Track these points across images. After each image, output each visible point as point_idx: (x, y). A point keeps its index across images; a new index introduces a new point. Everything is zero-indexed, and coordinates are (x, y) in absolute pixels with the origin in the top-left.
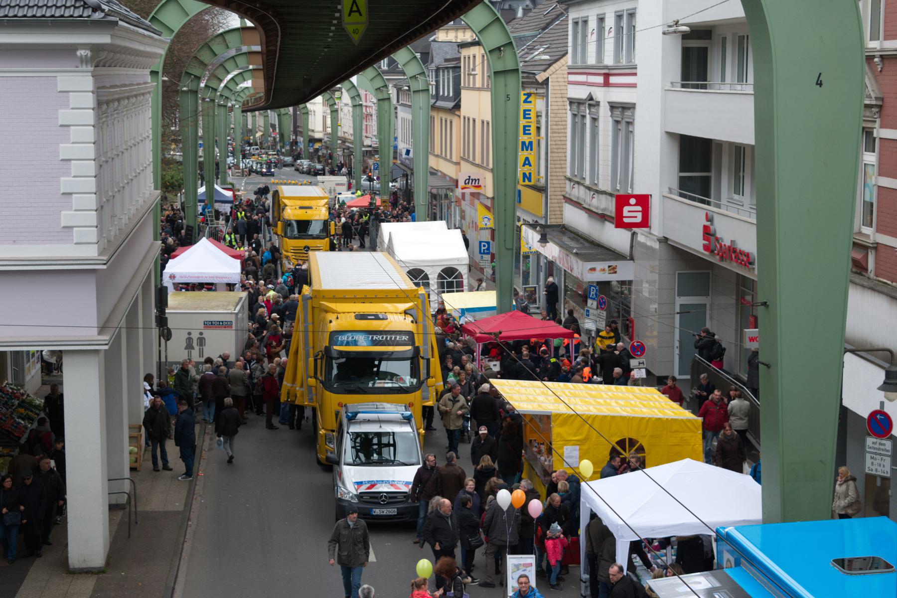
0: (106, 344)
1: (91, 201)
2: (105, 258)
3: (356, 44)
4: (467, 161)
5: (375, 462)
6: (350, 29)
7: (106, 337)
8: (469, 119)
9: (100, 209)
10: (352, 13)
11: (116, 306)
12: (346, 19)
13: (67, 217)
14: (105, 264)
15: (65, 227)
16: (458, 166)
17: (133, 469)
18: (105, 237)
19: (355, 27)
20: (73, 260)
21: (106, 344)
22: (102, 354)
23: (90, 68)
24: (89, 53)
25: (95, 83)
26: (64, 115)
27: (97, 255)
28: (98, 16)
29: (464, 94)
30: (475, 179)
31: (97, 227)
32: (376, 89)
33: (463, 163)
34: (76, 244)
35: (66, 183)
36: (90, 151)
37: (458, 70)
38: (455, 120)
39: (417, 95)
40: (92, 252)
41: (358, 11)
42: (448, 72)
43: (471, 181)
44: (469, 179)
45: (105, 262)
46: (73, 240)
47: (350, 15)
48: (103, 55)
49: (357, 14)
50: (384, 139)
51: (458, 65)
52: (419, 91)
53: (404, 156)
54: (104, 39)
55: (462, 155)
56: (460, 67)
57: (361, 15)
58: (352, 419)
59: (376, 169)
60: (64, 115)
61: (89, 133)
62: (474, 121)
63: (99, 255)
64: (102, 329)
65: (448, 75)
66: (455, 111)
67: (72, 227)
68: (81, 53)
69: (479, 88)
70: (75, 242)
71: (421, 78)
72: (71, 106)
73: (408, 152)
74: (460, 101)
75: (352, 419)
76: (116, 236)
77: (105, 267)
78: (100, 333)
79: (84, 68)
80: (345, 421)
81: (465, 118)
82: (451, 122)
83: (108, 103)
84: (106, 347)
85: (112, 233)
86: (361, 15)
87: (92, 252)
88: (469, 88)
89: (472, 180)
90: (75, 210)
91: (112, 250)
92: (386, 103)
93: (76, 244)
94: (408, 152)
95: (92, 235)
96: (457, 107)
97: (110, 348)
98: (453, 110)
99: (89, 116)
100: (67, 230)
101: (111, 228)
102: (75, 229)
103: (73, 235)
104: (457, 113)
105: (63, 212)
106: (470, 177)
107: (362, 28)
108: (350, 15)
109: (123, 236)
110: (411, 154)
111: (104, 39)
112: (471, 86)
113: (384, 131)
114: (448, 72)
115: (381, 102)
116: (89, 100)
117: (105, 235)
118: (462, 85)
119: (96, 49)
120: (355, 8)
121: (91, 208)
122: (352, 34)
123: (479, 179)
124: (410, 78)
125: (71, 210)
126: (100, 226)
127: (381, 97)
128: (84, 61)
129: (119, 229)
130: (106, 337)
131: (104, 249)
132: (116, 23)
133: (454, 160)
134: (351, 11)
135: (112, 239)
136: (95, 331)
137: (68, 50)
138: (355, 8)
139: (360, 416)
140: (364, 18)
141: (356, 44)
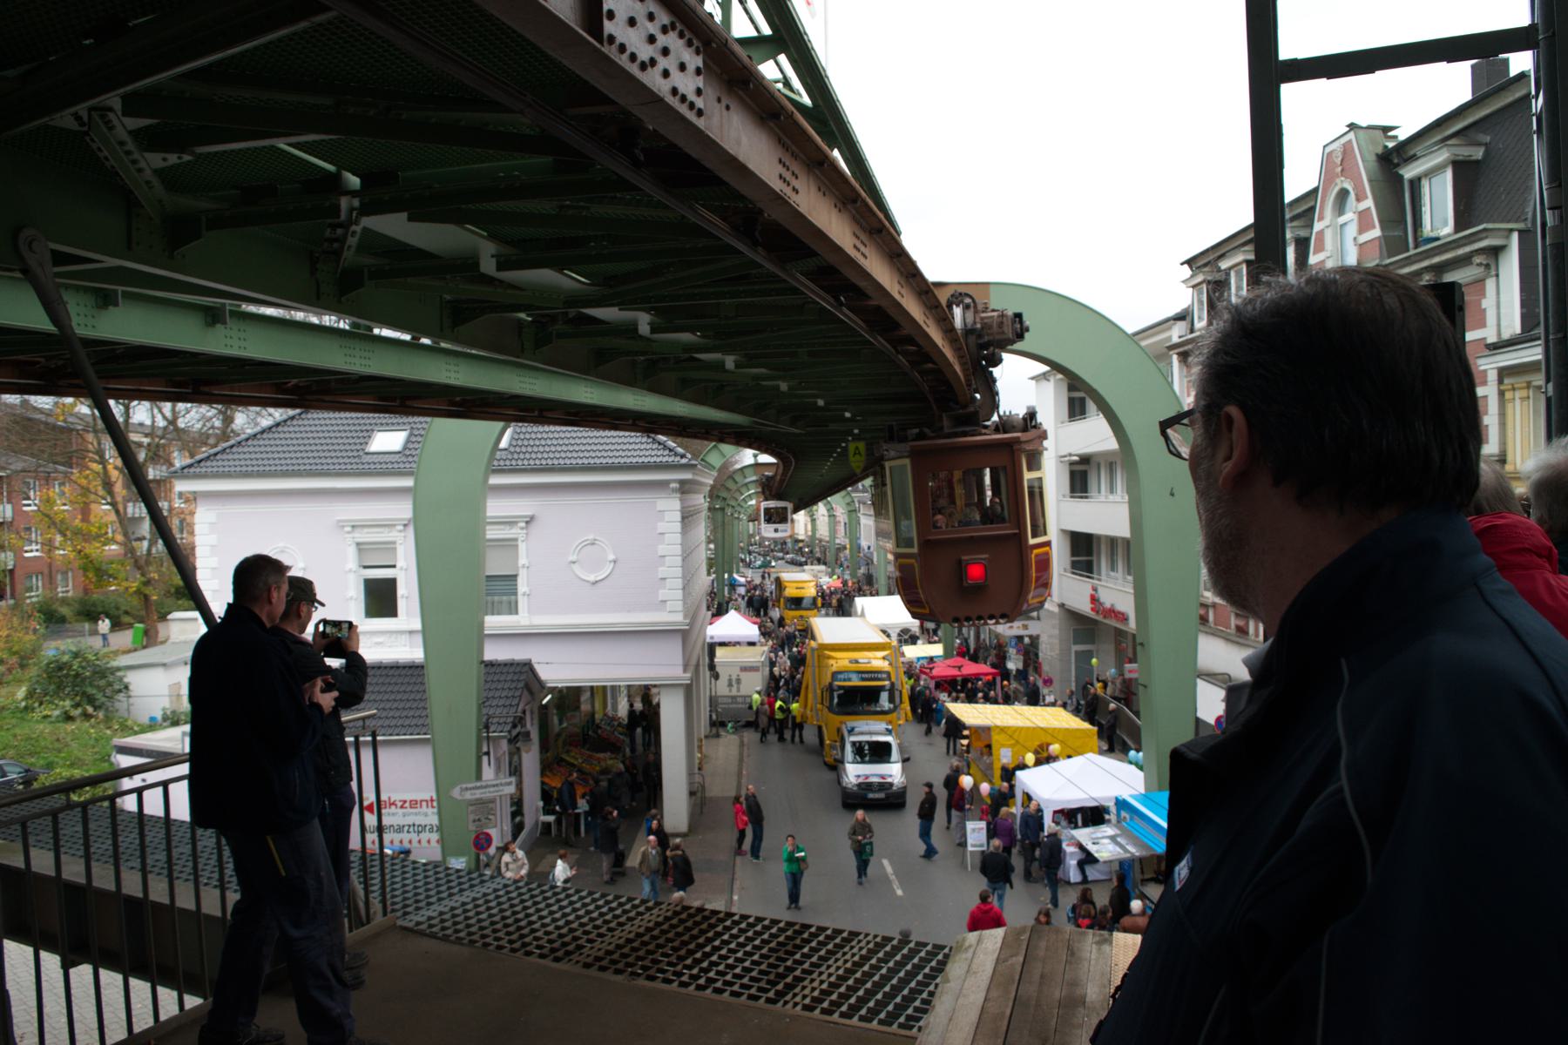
1: (679, 583)
9: (684, 589)
12: (852, 458)
13: (663, 594)
17: (700, 769)
23: (678, 495)
24: (678, 485)
25: (682, 504)
26: (662, 526)
28: (684, 461)
35: (662, 571)
36: (678, 550)
40: (679, 617)
41: (859, 453)
48: (687, 487)
54: (687, 476)
58: (851, 731)
60: (662, 526)
61: (678, 538)
68: (673, 485)
72: (666, 519)
73: (869, 548)
75: (851, 731)
79: (675, 495)
80: (846, 734)
83: (687, 517)
87: (679, 617)
94: (869, 548)
95: (679, 606)
99: (678, 527)
107: (862, 465)
110: (872, 549)
111: (687, 476)
116: (678, 516)
119: (682, 482)
126: (684, 600)
128: (674, 490)
130: (688, 675)
132: (696, 465)
134: (855, 454)
136: (681, 669)
137: (663, 485)
139: (856, 730)
140: (863, 458)
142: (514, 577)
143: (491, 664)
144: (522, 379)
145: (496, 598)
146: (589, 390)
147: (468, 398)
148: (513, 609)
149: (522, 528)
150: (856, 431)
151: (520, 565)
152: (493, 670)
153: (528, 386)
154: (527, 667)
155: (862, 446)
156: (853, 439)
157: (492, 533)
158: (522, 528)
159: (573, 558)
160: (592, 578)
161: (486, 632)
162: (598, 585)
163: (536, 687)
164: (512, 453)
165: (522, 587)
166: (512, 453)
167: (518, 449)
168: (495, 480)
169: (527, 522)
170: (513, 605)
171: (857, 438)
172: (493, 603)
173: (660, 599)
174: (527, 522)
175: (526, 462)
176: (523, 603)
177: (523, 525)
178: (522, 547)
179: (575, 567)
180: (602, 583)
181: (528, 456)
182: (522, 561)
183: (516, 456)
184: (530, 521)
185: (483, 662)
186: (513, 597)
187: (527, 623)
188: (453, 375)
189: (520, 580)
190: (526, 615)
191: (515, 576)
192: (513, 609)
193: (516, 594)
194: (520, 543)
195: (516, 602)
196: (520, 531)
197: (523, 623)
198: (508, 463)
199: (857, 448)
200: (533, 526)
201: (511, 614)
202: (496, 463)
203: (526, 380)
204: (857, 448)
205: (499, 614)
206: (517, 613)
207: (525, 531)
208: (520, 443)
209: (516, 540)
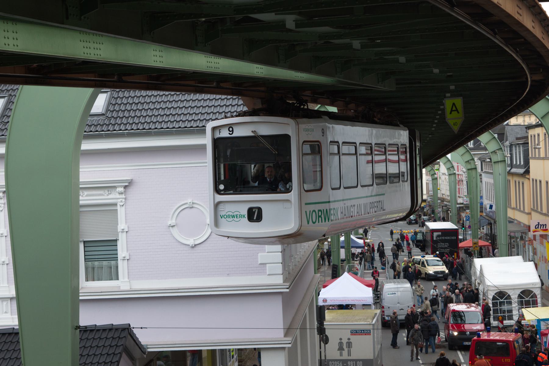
0: (289, 343)
2: (288, 284)
3: (456, 132)
4: (536, 211)
5: (525, 213)
6: (451, 122)
7: (289, 339)
8: (536, 181)
10: (453, 112)
11: (294, 318)
12: (448, 116)
14: (287, 288)
15: (261, 264)
16: (530, 216)
18: (286, 270)
19: (454, 121)
20: (267, 286)
21: (289, 343)
22: (287, 349)
27: (282, 282)
29: (532, 163)
30: (543, 225)
31: (282, 263)
32: (466, 162)
33: (533, 213)
34: (268, 275)
37: (526, 145)
38: (526, 182)
39: (497, 165)
40: (279, 280)
41: (457, 110)
42: (519, 147)
43: (540, 226)
44: (538, 225)
45: (288, 287)
46: (266, 272)
47: (451, 113)
49: (456, 112)
50: (473, 198)
51: (527, 142)
52: (498, 162)
53: (488, 210)
55: (532, 207)
56: (528, 143)
57: (458, 112)
59: (468, 220)
62: (540, 182)
63: (284, 283)
64: (288, 331)
65: (519, 149)
66: (525, 175)
67: (266, 264)
69: (543, 158)
70: (268, 273)
71: (499, 153)
73: (491, 207)
74: (529, 167)
76: (293, 269)
77: (288, 290)
78: (286, 335)
81: (533, 180)
82: (523, 184)
84: (290, 346)
85: (291, 268)
86: (458, 112)
88: (535, 158)
89: (541, 225)
90: (268, 252)
91: (292, 278)
92: (474, 171)
93: (268, 275)
94: (491, 207)
95: (279, 269)
96: (527, 172)
97: (292, 346)
98: (524, 174)
100: (262, 266)
101: (290, 264)
102: (267, 265)
103: (266, 269)
104: (527, 176)
105: (259, 254)
106: (539, 223)
107: (459, 122)
108: (451, 113)
109: (298, 270)
112: (537, 156)
113: (473, 192)
114: (519, 147)
115: (470, 171)
117: (286, 269)
118: (530, 156)
120: (454, 109)
121: (278, 251)
122: (453, 126)
123: (546, 225)
124: (491, 153)
125: (265, 252)
126: (284, 263)
127: (469, 167)
129: (295, 265)
131: (287, 278)
133: (526, 211)
134: (452, 111)
135: (291, 272)
138: (454, 109)
140: (461, 115)
141: (456, 132)
142: (114, 242)
143: (86, 330)
144: (86, 44)
145: (96, 263)
146: (158, 53)
147: (44, 64)
148: (113, 275)
149: (121, 193)
150: (452, 87)
151: (119, 230)
152: (85, 336)
153: (92, 51)
154: (127, 330)
155: (459, 102)
156: (453, 96)
157: (85, 198)
158: (121, 193)
159: (172, 222)
160: (191, 242)
161: (81, 298)
162: (195, 249)
163: (137, 354)
164: (109, 118)
165: (122, 252)
166: (109, 118)
167: (115, 114)
168: (86, 146)
169: (125, 187)
170: (113, 270)
171: (454, 95)
172: (93, 268)
173: (259, 263)
174: (125, 187)
175: (123, 127)
176: (122, 266)
177: (121, 189)
178: (121, 212)
179: (175, 231)
180: (201, 245)
181: (124, 121)
182: (122, 225)
183: (113, 121)
184: (128, 185)
185: (78, 327)
186: (113, 263)
187: (127, 288)
188: (11, 42)
189: (119, 243)
190: (127, 279)
191: (116, 241)
192: (113, 275)
193: (116, 259)
194: (118, 207)
195: (117, 267)
196: (118, 196)
197: (122, 288)
198: (105, 128)
199: (454, 104)
200: (130, 190)
201: (111, 279)
202: (87, 129)
203: (92, 45)
204: (454, 104)
205: (99, 280)
206: (118, 279)
207: (123, 196)
208: (117, 107)
209: (115, 205)
